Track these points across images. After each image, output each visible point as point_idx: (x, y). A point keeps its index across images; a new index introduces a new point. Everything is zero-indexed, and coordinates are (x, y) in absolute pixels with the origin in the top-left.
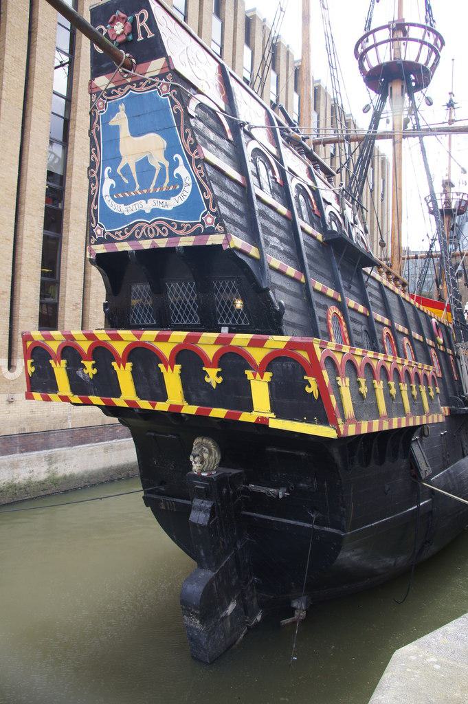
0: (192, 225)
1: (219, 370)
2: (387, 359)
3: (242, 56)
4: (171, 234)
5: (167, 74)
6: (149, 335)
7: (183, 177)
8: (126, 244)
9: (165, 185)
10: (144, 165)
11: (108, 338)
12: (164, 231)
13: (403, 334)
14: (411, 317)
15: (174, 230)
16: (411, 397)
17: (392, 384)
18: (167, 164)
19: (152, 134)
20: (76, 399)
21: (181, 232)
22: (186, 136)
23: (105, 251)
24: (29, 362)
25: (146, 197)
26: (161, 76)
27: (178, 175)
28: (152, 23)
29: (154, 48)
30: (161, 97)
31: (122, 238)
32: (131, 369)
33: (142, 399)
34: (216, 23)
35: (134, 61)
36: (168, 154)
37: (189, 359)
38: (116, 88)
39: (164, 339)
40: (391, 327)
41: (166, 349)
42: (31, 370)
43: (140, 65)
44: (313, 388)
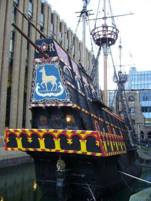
0: (63, 101)
1: (72, 140)
2: (109, 135)
3: (50, 27)
4: (57, 103)
5: (58, 61)
6: (51, 130)
7: (61, 88)
8: (42, 104)
9: (56, 90)
10: (49, 84)
11: (38, 131)
12: (55, 102)
13: (112, 126)
14: (114, 121)
15: (58, 102)
16: (118, 146)
17: (108, 142)
18: (56, 84)
19: (52, 76)
20: (24, 149)
21: (60, 102)
22: (63, 77)
23: (35, 106)
24: (8, 138)
25: (49, 92)
26: (56, 61)
27: (59, 87)
28: (54, 47)
29: (55, 54)
30: (56, 66)
31: (41, 103)
32: (60, 140)
33: (47, 148)
34: (42, 16)
35: (48, 56)
36: (57, 82)
37: (63, 137)
38: (42, 62)
39: (55, 132)
40: (110, 125)
42: (8, 141)
43: (50, 57)
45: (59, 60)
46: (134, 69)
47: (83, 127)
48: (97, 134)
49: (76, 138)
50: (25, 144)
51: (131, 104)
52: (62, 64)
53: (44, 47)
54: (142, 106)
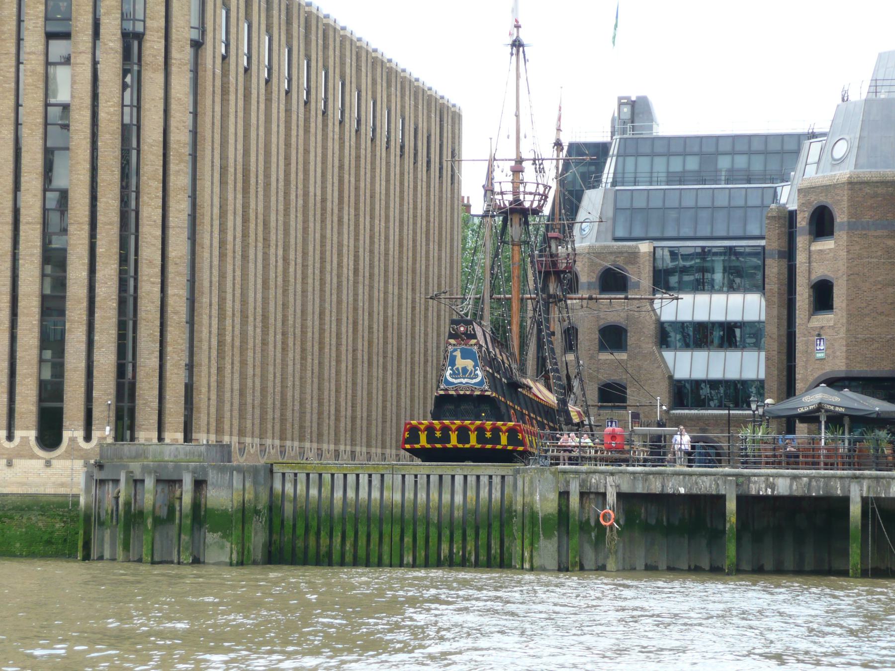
14: (536, 409)
28: (473, 329)
36: (474, 367)
37: (481, 430)
40: (529, 415)
41: (472, 427)
42: (407, 436)
44: (520, 437)
45: (477, 344)
46: (636, 111)
48: (520, 426)
49: (496, 431)
50: (431, 438)
52: (481, 347)
53: (462, 329)
54: (664, 318)
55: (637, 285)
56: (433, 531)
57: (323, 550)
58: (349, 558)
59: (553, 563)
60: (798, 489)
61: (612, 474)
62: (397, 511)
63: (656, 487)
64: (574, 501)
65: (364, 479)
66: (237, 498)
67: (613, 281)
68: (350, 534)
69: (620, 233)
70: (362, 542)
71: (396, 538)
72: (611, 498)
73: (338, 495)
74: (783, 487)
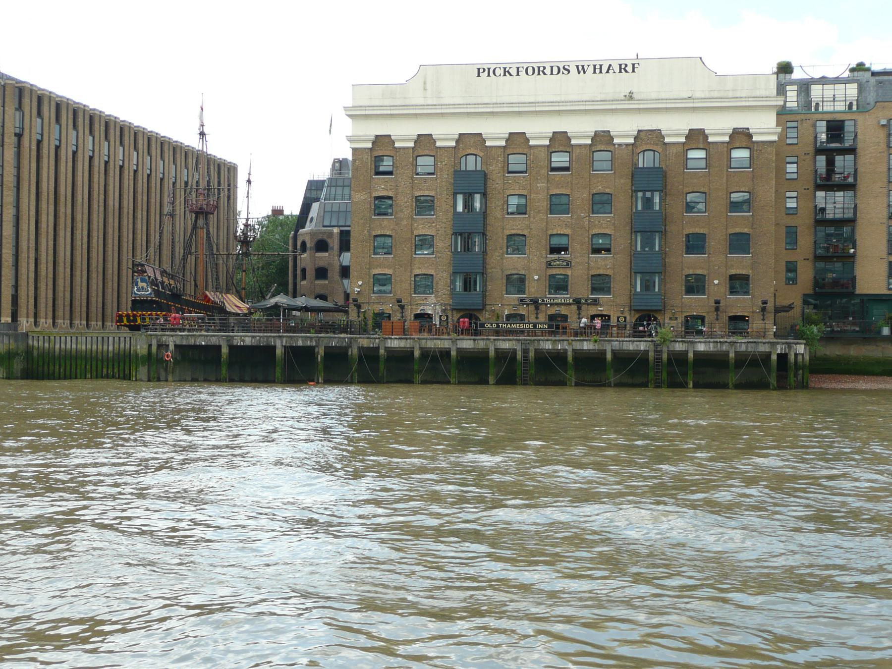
47: (162, 311)
50: (128, 320)
51: (320, 258)
55: (332, 248)
56: (100, 363)
57: (51, 372)
58: (62, 375)
59: (145, 377)
60: (254, 342)
61: (172, 336)
62: (83, 354)
63: (192, 342)
64: (154, 349)
65: (69, 339)
66: (6, 347)
67: (322, 246)
68: (63, 364)
69: (327, 223)
70: (68, 368)
71: (83, 366)
72: (172, 347)
73: (57, 346)
74: (248, 341)
